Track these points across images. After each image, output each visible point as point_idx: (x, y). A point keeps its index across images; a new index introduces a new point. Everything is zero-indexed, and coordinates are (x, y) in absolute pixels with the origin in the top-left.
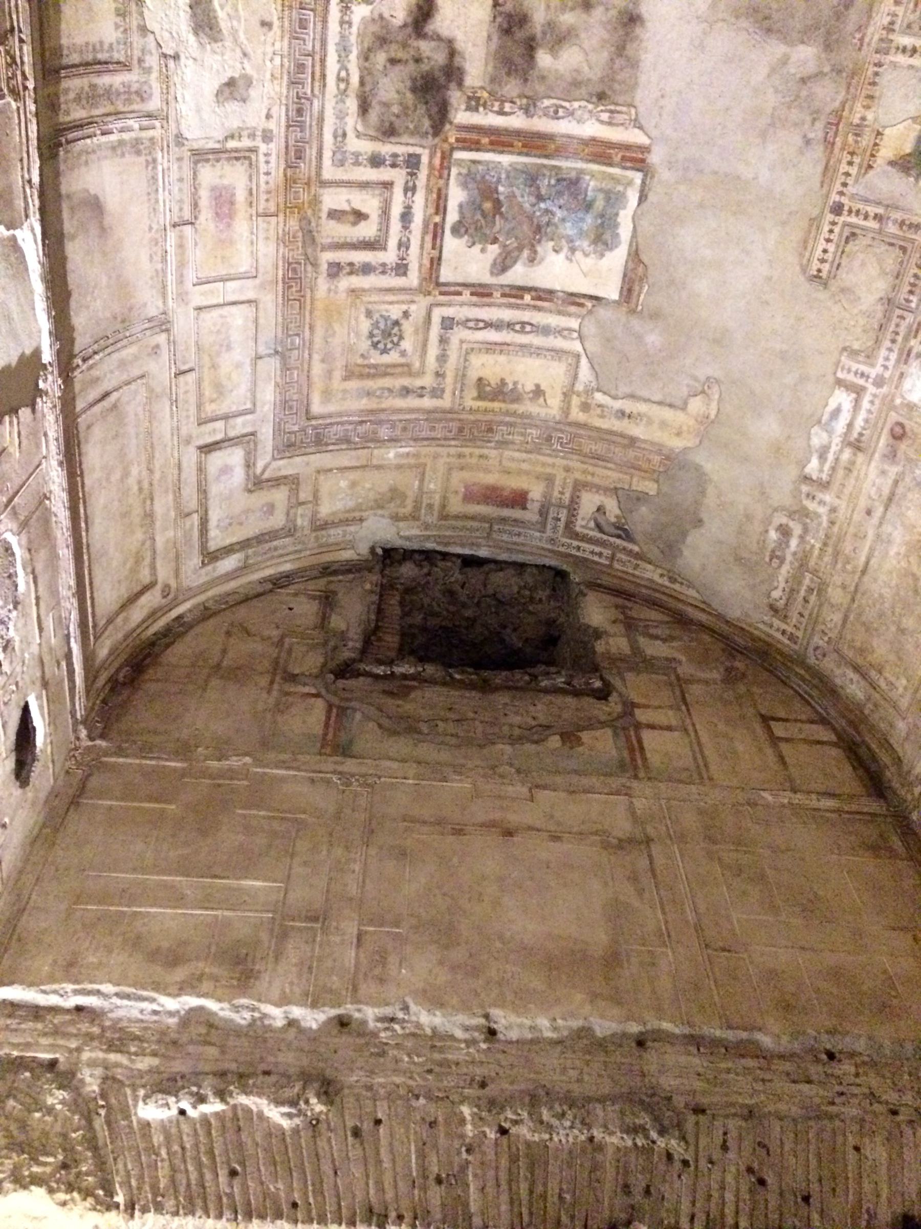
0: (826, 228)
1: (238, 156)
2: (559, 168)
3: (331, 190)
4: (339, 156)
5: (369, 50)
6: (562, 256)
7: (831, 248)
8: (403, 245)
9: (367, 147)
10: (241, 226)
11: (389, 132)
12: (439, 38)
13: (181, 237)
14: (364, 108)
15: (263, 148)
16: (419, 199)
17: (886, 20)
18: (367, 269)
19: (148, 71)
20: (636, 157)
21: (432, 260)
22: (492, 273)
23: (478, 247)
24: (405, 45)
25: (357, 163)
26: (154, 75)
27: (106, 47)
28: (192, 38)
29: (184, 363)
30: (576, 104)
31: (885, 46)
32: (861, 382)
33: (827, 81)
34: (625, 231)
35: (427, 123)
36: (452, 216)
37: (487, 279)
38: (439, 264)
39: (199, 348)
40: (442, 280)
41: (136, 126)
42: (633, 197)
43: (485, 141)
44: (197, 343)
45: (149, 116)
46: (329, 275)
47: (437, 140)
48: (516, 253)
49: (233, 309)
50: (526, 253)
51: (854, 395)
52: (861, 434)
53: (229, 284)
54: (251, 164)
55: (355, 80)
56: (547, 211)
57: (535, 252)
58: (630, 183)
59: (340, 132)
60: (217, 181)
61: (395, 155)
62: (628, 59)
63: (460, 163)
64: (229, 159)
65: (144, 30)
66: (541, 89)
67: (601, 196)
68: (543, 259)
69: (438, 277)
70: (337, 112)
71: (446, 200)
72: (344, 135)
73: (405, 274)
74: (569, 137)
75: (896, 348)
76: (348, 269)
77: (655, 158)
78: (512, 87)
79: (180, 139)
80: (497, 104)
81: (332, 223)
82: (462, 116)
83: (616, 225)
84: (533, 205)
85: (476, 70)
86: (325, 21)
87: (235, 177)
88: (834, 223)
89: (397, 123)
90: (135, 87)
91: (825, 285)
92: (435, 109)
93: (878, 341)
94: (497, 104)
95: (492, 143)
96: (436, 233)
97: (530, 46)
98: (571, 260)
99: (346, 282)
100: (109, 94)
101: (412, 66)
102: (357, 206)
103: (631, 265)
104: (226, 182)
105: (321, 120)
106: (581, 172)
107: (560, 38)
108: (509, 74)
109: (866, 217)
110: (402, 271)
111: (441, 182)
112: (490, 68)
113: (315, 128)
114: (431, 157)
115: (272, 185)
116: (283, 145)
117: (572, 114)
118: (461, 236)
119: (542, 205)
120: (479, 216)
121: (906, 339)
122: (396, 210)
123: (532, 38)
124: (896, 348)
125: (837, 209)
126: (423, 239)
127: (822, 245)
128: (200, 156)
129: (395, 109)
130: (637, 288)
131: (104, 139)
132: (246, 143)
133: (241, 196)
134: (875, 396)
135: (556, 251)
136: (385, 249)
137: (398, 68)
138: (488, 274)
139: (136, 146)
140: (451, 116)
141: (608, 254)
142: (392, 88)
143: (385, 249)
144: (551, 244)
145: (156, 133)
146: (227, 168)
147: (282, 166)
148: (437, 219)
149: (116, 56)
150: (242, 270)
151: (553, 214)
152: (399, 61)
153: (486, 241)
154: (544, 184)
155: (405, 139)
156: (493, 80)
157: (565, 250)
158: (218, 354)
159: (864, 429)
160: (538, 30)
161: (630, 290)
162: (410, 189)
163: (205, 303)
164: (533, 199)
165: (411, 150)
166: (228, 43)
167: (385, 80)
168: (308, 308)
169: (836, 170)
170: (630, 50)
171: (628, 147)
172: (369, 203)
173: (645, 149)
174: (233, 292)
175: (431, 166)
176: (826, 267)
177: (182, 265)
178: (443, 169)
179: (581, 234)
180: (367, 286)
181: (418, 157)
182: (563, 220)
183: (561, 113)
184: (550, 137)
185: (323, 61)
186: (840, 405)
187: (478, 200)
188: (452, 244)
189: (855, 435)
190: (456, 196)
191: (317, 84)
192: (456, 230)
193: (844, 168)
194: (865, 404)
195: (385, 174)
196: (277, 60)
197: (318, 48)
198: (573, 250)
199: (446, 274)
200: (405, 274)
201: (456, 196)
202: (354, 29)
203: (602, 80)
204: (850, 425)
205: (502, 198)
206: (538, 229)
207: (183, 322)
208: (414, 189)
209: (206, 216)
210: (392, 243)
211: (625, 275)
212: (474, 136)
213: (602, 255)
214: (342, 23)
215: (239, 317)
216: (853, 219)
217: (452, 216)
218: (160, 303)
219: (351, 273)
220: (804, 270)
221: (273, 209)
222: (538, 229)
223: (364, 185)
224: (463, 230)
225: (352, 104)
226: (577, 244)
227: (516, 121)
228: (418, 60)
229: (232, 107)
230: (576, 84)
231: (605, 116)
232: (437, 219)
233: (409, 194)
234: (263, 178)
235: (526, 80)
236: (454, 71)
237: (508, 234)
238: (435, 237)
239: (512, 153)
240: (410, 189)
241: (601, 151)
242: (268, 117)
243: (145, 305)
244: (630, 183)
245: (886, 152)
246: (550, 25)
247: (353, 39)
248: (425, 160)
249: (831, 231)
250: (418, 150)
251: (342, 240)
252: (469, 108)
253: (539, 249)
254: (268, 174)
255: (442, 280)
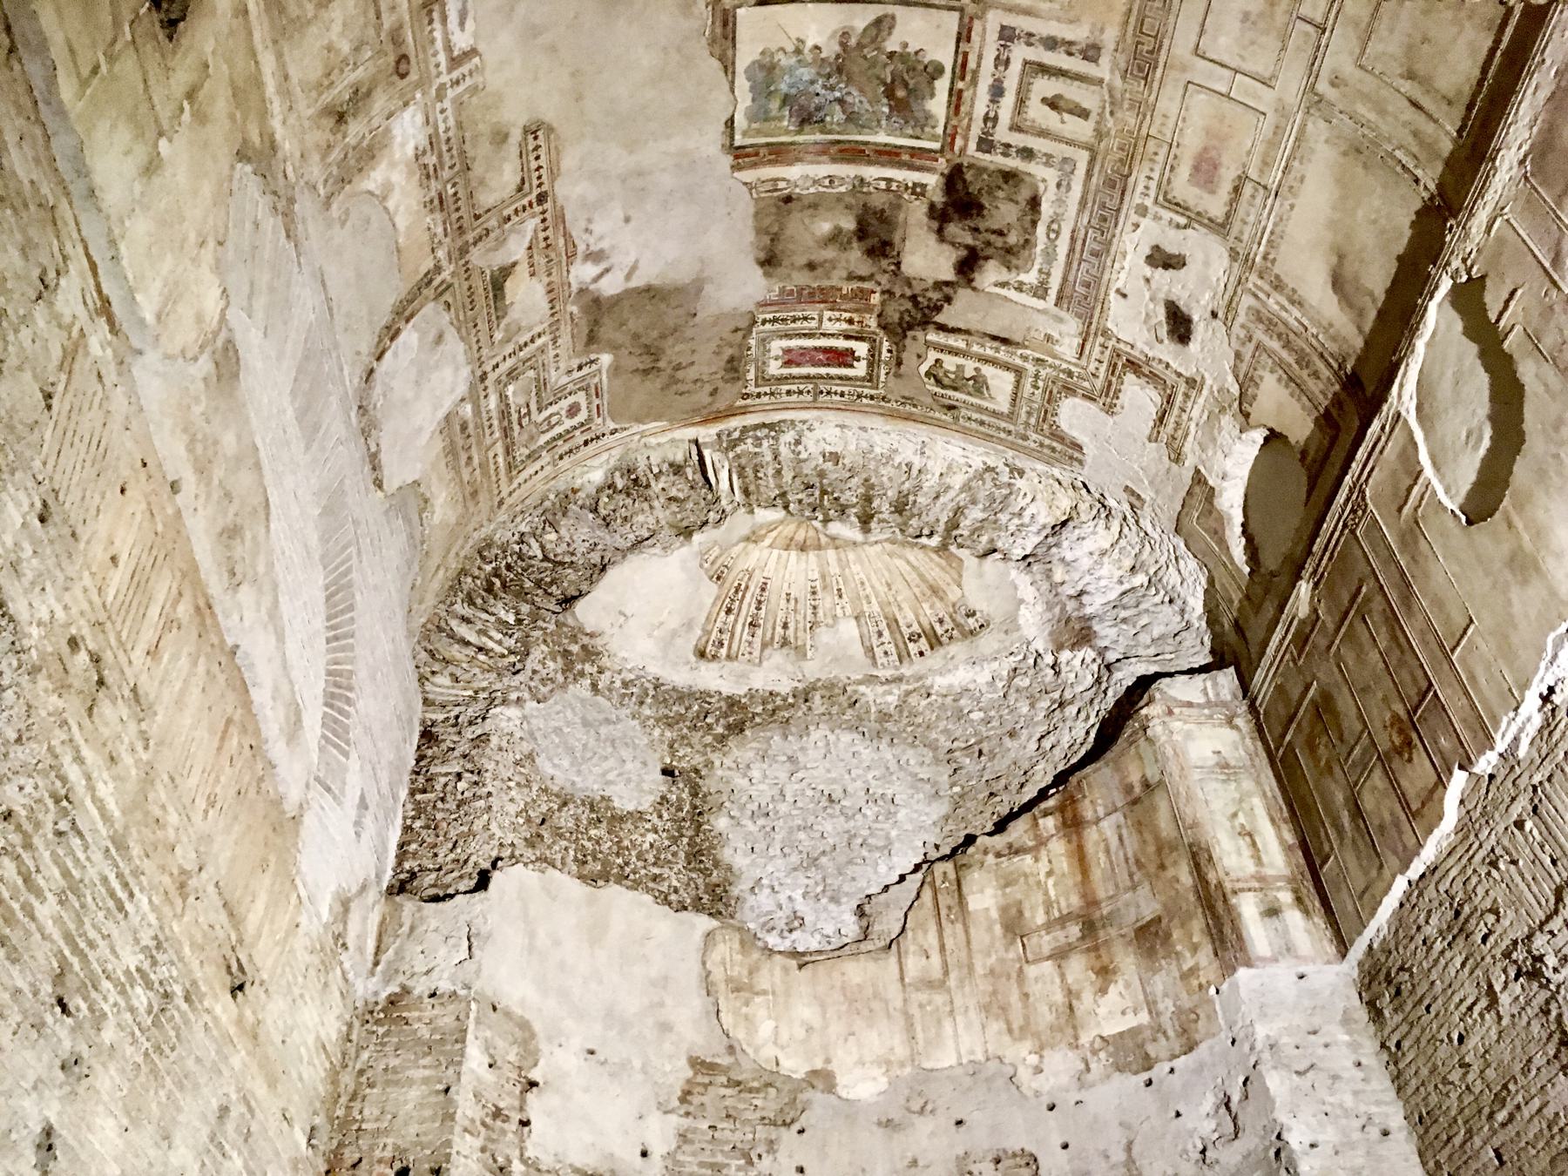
0: (544, 178)
1: (1178, 206)
2: (822, 132)
3: (1084, 139)
4: (1068, 168)
5: (1024, 247)
6: (810, 44)
7: (534, 164)
8: (1002, 62)
9: (1035, 169)
10: (1192, 142)
11: (1009, 176)
12: (953, 244)
13: (1261, 171)
14: (1034, 203)
15: (1149, 202)
16: (981, 107)
17: (560, 341)
18: (1051, 43)
19: (1243, 326)
20: (742, 156)
21: (969, 40)
22: (893, 17)
23: (911, 49)
24: (988, 244)
25: (1049, 156)
26: (1241, 319)
27: (1276, 376)
28: (1195, 318)
29: (1307, 34)
30: (812, 190)
31: (554, 327)
32: (455, 74)
33: (588, 280)
34: (742, 83)
35: (969, 176)
36: (942, 85)
37: (899, 11)
38: (959, 33)
39: (1284, 39)
40: (956, 15)
41: (1271, 301)
42: (740, 122)
43: (905, 157)
44: (1284, 49)
45: (1256, 296)
46: (1099, 49)
47: (958, 161)
48: (866, 41)
49: (1226, 59)
50: (853, 42)
51: (456, 53)
52: (431, 22)
53: (1224, 90)
54: (1166, 193)
55: (1041, 230)
56: (832, 89)
57: (843, 45)
58: (745, 134)
59: (1063, 189)
60: (1206, 196)
61: (1005, 155)
62: (767, 233)
63: (934, 138)
64: (1187, 209)
65: (1238, 355)
66: (850, 200)
67: (774, 113)
68: (832, 36)
69: (961, 19)
70: (1064, 205)
71: (949, 103)
72: (1059, 185)
73: (1003, 28)
74: (819, 163)
75: (443, 137)
76: (1074, 49)
77: (728, 160)
78: (878, 201)
79: (1234, 255)
80: (894, 188)
81: (1085, 105)
82: (932, 180)
83: (752, 89)
84: (849, 93)
85: (916, 212)
86: (1065, 279)
87: (1183, 188)
88: (539, 186)
89: (1000, 181)
90: (1261, 326)
91: (526, 131)
92: (960, 186)
93: (460, 125)
94: (894, 188)
95: (897, 155)
96: (961, 69)
97: (862, 233)
98: (799, 40)
99: (1079, 34)
100: (1287, 345)
101: (982, 225)
102: (1054, 114)
103: (730, 53)
104: (1197, 191)
105: (1083, 203)
106: (799, 132)
107: (835, 237)
108: (883, 211)
109: (516, 211)
110: (1007, 33)
111: (954, 122)
112: (901, 217)
113: (1090, 198)
114: (963, 150)
115: (1146, 165)
116: (1127, 198)
117: (815, 182)
118: (931, 62)
119: (838, 94)
120: (912, 83)
121: (440, 156)
122: (1008, 101)
123: (860, 239)
124: (443, 137)
125: (541, 198)
126: (979, 65)
127: (542, 162)
128: (1220, 227)
129: (1001, 194)
130: (719, 30)
131: (1306, 323)
132: (1167, 215)
133: (1184, 171)
134: (439, 74)
135: (817, 47)
136: (1026, 63)
137: (996, 227)
138: (898, 20)
139: (1278, 285)
140: (942, 180)
141: (757, 57)
142: (1004, 212)
143: (1026, 63)
144: (823, 55)
145: (1253, 278)
146: (1191, 203)
147: (1132, 180)
148: (960, 85)
149: (1270, 361)
150: (1202, 96)
151: (824, 87)
152: (994, 232)
153: (901, 55)
154: (838, 115)
155: (992, 167)
156: (899, 207)
157: (806, 51)
158: (1261, 15)
159: (431, 32)
160: (855, 245)
161: (725, 24)
162: (991, 119)
163: (1259, 85)
164: (849, 99)
165: (987, 157)
166: (1162, 296)
167: (1009, 220)
168: (1132, 20)
169: (556, 227)
170: (766, 240)
171: (754, 165)
172: (1037, 112)
173: (736, 168)
174: (1221, 78)
175: (966, 139)
176: (531, 144)
177: (1273, 144)
178: (950, 137)
179: (791, 70)
180: (1054, 23)
181: (979, 149)
182: (812, 82)
183: (827, 182)
184: (834, 160)
185: (1072, 250)
186: (463, 30)
187: (911, 100)
188: (944, 55)
189: (436, 15)
190: (938, 105)
191: (1082, 235)
192: (939, 70)
193: (549, 233)
194: (442, 58)
195: (1018, 140)
196: (1117, 265)
197: (1075, 266)
198: (798, 51)
199: (951, 21)
200: (1003, 28)
201: (938, 105)
202: (1037, 267)
203: (789, 212)
204: (444, 19)
205: (885, 101)
206: (840, 70)
207: (1291, 84)
208: (986, 119)
209: (1228, 176)
210: (1016, 67)
211: (734, 38)
212: (918, 162)
213: (763, 53)
214: (1048, 274)
215: (1223, 44)
216: (525, 202)
217: (942, 85)
218: (1310, 126)
219: (1071, 43)
220: (551, 129)
221: (1151, 143)
222: (840, 70)
223: (1043, 133)
224: (930, 69)
225: (1046, 208)
226: (793, 60)
227: (871, 172)
228: (976, 230)
229: (1172, 249)
230: (814, 206)
231: (781, 185)
232: (960, 85)
233: (992, 115)
234: (1156, 175)
235: (864, 205)
236: (939, 217)
237: (873, 63)
238: (964, 65)
239: (875, 144)
240: (991, 119)
241: (780, 153)
242: (1137, 226)
243: (1327, 141)
244: (745, 134)
245: (522, 270)
246: (845, 247)
247: (1039, 260)
248: (972, 146)
249: (539, 177)
250: (979, 155)
251: (1077, 83)
252: (924, 186)
253: (837, 48)
254: (1149, 178)
255: (956, 15)
